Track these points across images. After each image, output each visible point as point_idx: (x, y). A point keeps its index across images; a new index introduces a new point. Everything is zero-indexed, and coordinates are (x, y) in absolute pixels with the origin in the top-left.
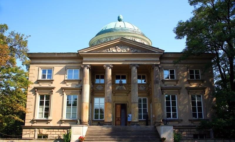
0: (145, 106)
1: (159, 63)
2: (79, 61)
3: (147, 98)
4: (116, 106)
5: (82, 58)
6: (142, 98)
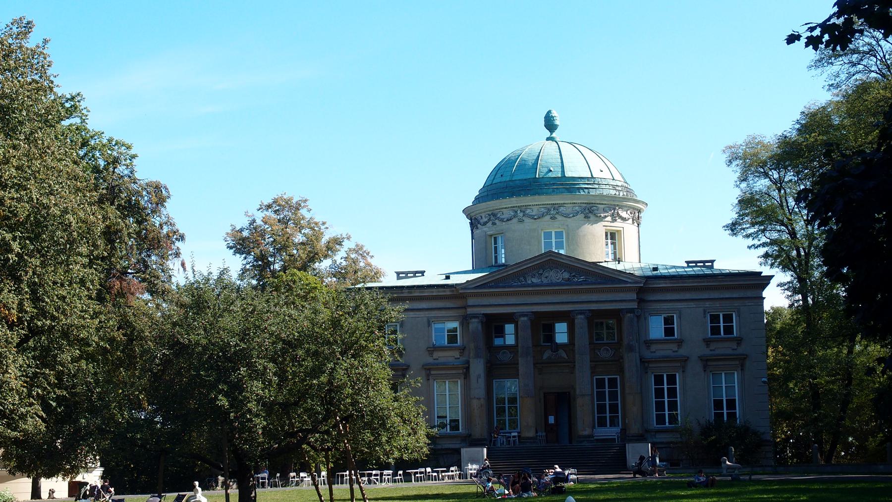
0: (613, 395)
1: (634, 305)
2: (459, 303)
6: (606, 378)
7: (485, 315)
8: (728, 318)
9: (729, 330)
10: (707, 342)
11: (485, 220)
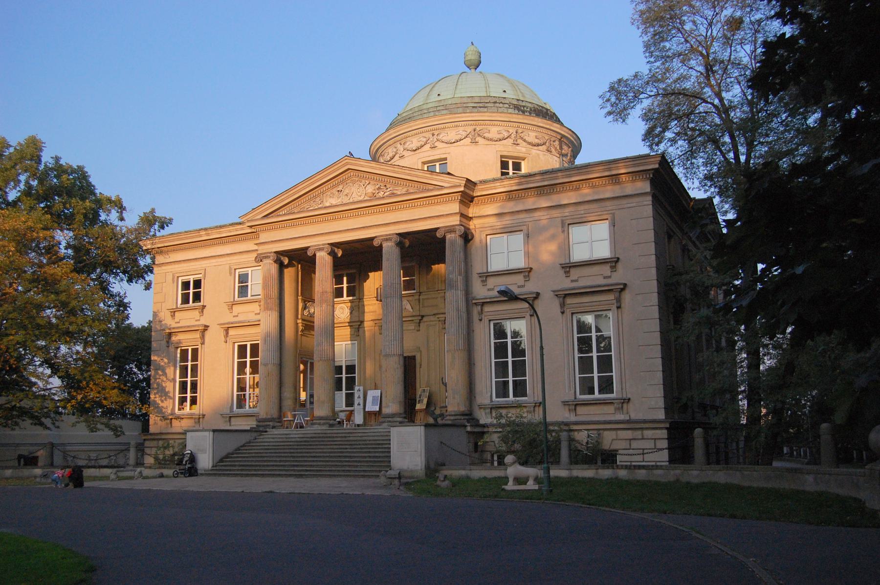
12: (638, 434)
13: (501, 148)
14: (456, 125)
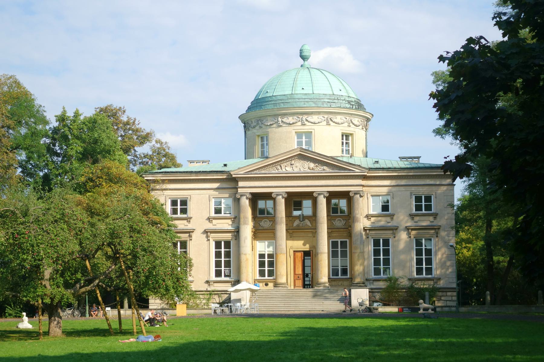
3: (348, 240)
4: (294, 255)
5: (237, 182)
7: (252, 194)
8: (428, 199)
9: (428, 208)
10: (412, 216)
11: (254, 124)
12: (444, 294)
13: (342, 128)
14: (319, 113)
